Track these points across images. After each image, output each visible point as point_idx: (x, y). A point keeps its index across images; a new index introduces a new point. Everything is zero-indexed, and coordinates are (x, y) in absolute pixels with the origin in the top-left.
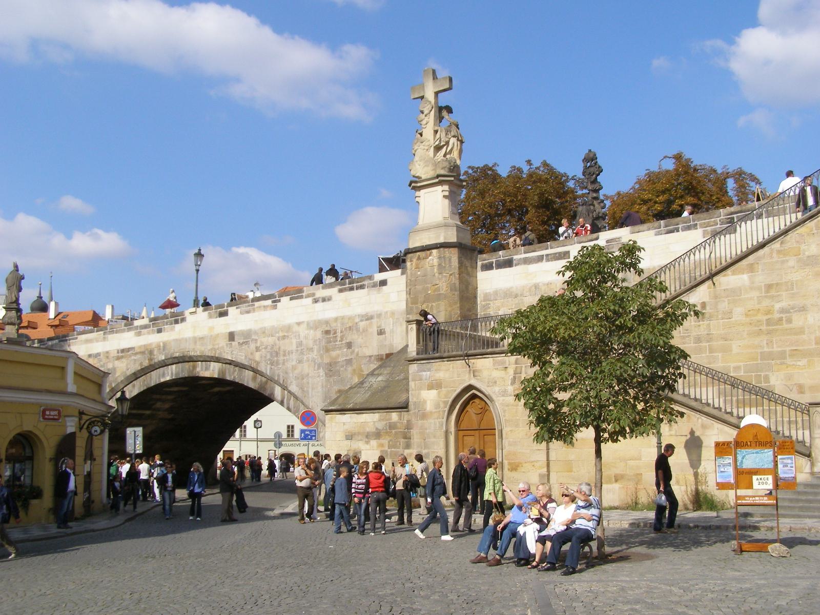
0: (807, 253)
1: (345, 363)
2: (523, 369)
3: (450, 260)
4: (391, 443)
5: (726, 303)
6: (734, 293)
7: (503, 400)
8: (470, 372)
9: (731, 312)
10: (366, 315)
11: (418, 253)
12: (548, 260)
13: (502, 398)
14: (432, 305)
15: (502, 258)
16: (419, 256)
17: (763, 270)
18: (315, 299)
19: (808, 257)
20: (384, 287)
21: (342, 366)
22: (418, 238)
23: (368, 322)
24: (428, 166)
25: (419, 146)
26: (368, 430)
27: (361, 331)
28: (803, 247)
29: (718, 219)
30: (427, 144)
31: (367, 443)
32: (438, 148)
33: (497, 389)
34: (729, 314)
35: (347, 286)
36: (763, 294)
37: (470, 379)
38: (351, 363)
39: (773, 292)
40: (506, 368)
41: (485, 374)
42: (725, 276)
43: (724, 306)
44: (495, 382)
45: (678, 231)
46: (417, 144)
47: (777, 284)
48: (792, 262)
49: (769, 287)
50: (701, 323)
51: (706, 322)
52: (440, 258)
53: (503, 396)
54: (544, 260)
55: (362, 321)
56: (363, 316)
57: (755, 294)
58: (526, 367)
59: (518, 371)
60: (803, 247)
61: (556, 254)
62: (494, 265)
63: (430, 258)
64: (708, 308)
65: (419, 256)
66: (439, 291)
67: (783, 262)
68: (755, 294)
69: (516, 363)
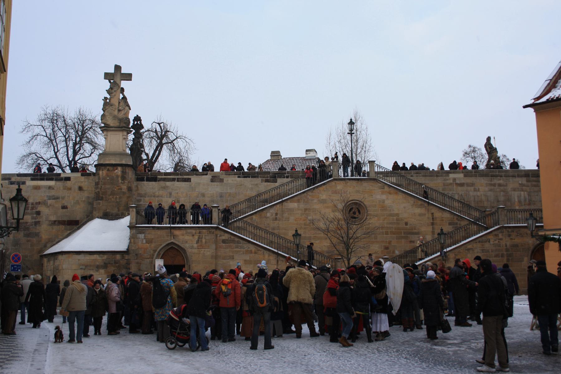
0: (322, 198)
1: (34, 223)
2: (204, 236)
3: (128, 174)
4: (115, 271)
5: (287, 214)
6: (291, 210)
7: (191, 251)
8: (171, 236)
9: (289, 219)
10: (54, 196)
11: (108, 167)
12: (178, 181)
13: (190, 250)
14: (116, 197)
15: (150, 176)
16: (108, 169)
17: (303, 203)
18: (11, 182)
19: (322, 199)
20: (68, 182)
21: (32, 225)
22: (107, 159)
23: (54, 201)
24: (115, 120)
25: (109, 107)
26: (98, 263)
27: (48, 205)
28: (320, 195)
29: (269, 175)
30: (115, 107)
31: (97, 271)
32: (119, 111)
33: (187, 245)
34: (288, 219)
35: (39, 177)
36: (303, 212)
37: (171, 239)
38: (40, 223)
39: (307, 212)
40: (193, 235)
41: (181, 237)
42: (287, 202)
43: (286, 215)
44: (187, 242)
45: (249, 177)
46: (108, 106)
47: (309, 209)
48: (315, 201)
49: (306, 210)
50: (275, 221)
51: (277, 222)
52: (123, 172)
53: (191, 249)
54: (176, 181)
55: (50, 199)
56: (50, 197)
57: (300, 212)
58: (205, 235)
59: (201, 237)
60: (320, 195)
61: (183, 178)
62: (145, 179)
63: (116, 171)
64: (278, 215)
65: (108, 169)
66: (122, 190)
67: (312, 200)
68: (300, 212)
69: (200, 233)
